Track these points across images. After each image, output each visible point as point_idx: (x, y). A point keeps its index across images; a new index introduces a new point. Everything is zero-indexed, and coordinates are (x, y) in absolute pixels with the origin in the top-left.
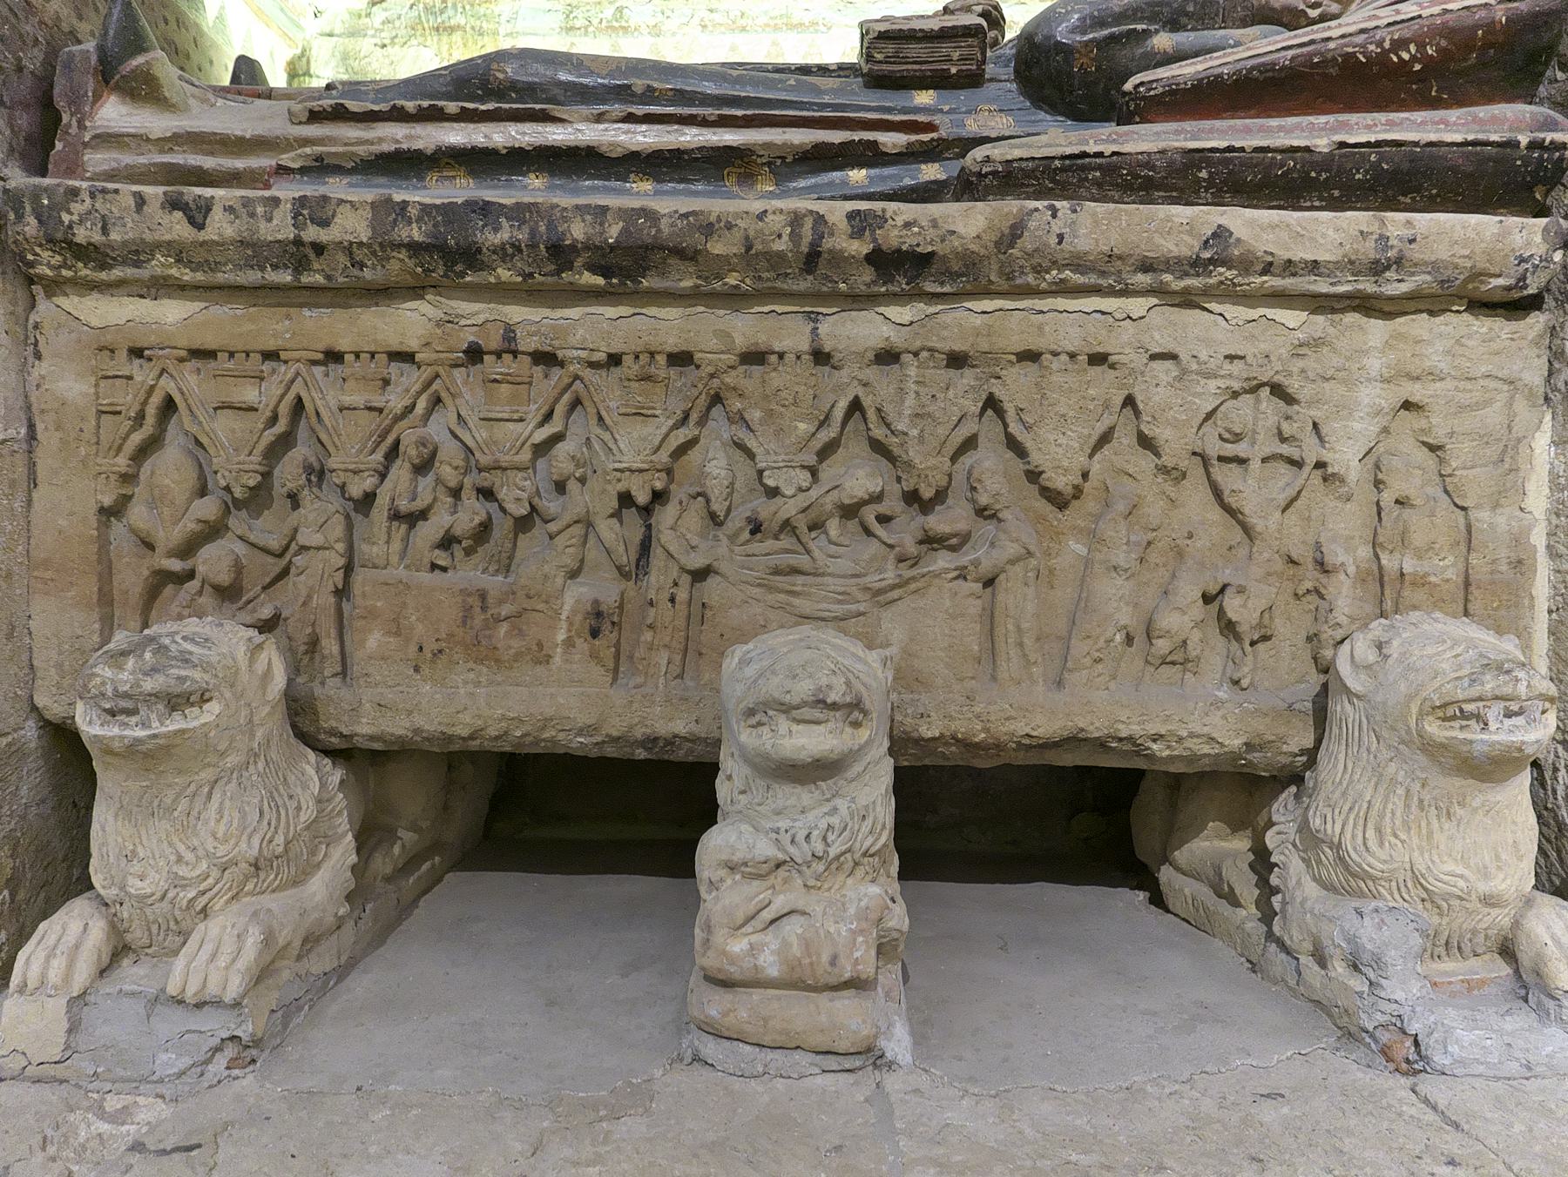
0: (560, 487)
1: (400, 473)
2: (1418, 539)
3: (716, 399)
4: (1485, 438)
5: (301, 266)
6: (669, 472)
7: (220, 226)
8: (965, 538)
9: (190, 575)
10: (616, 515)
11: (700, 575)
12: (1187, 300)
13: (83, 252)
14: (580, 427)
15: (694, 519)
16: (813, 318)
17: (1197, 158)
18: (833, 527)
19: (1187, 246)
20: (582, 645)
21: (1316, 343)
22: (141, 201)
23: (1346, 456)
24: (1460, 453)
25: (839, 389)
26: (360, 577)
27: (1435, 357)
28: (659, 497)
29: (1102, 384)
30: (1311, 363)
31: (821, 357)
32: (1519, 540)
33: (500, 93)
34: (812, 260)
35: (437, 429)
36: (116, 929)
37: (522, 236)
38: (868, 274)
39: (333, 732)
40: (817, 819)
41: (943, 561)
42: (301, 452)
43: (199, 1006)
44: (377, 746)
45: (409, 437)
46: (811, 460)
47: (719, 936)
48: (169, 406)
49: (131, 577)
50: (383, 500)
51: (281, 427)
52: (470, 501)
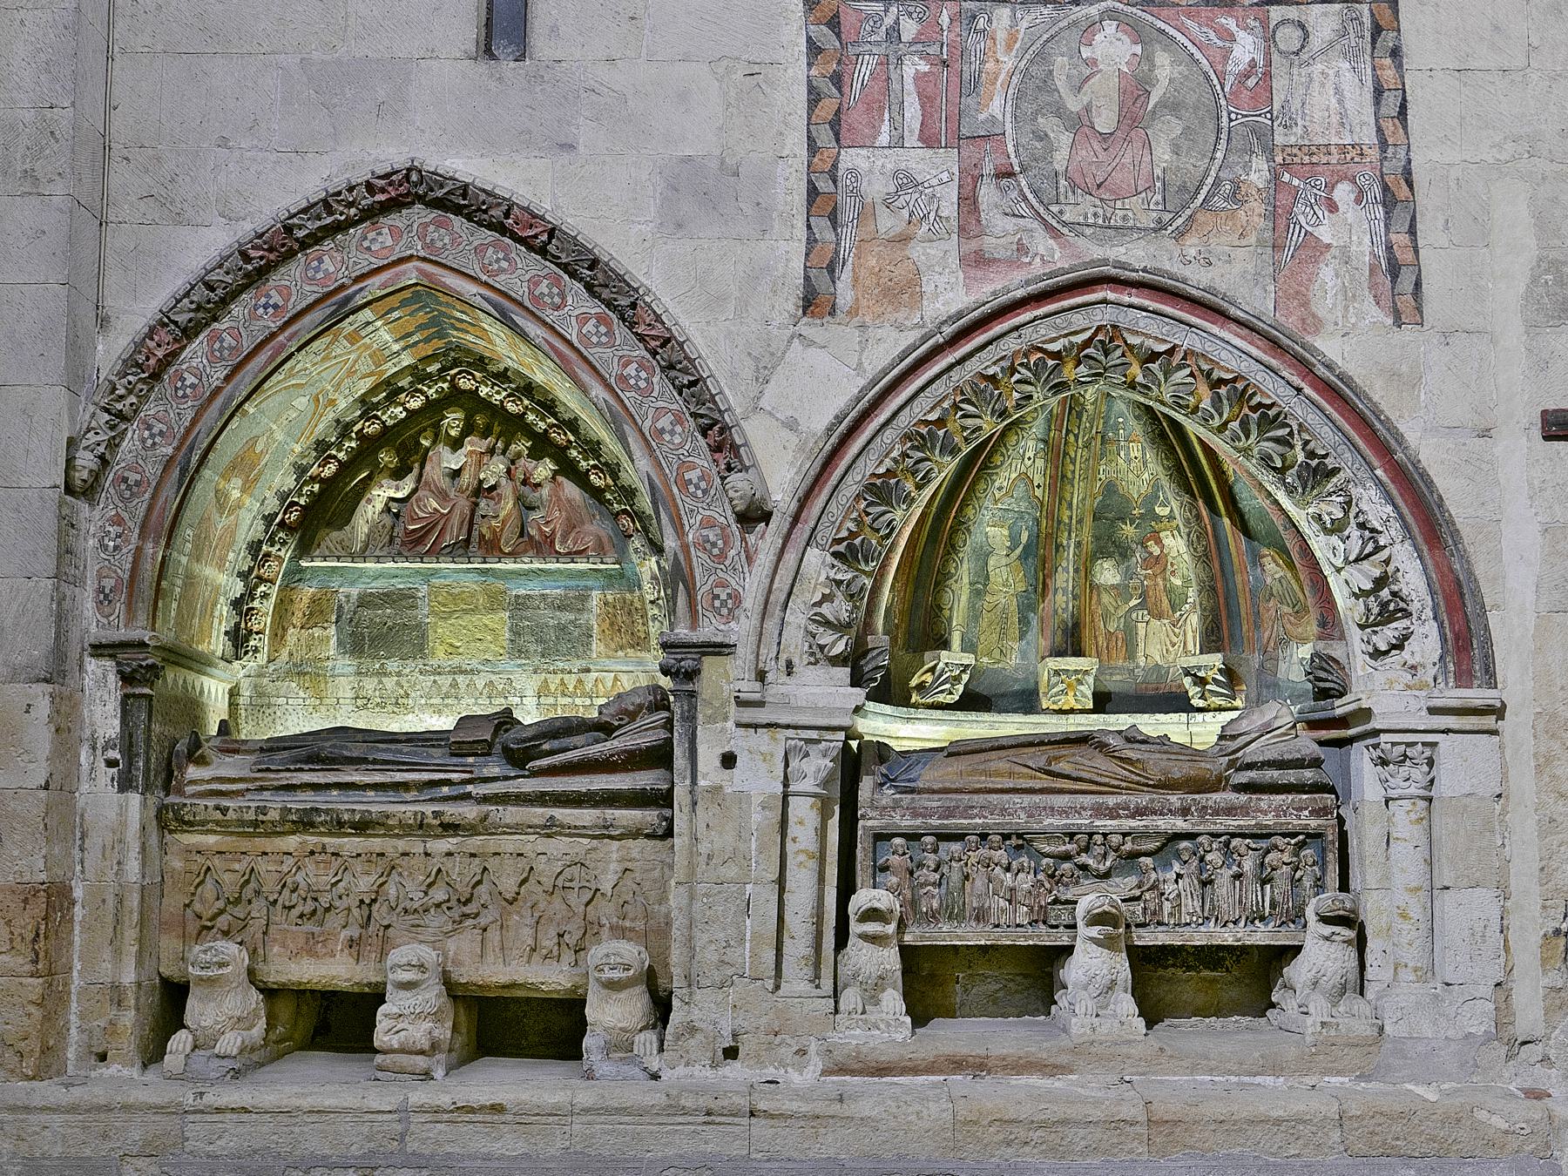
0: (340, 897)
1: (286, 892)
2: (631, 915)
3: (393, 868)
4: (655, 881)
5: (256, 826)
6: (377, 892)
7: (231, 815)
8: (477, 915)
9: (213, 927)
10: (359, 907)
11: (387, 927)
12: (549, 836)
13: (186, 823)
14: (348, 877)
15: (385, 908)
16: (425, 842)
17: (543, 794)
18: (432, 910)
19: (542, 821)
20: (346, 951)
21: (595, 849)
22: (206, 807)
23: (606, 887)
24: (647, 885)
25: (434, 865)
26: (272, 928)
27: (635, 854)
28: (374, 901)
29: (522, 862)
30: (593, 855)
31: (427, 854)
32: (668, 915)
33: (322, 761)
34: (421, 826)
35: (299, 877)
36: (195, 1040)
37: (328, 819)
38: (440, 829)
39: (261, 981)
40: (412, 1001)
41: (469, 922)
42: (253, 885)
43: (223, 1058)
44: (275, 987)
45: (289, 880)
46: (424, 888)
47: (381, 1035)
48: (209, 869)
49: (193, 927)
50: (280, 902)
51: (246, 877)
52: (309, 901)
